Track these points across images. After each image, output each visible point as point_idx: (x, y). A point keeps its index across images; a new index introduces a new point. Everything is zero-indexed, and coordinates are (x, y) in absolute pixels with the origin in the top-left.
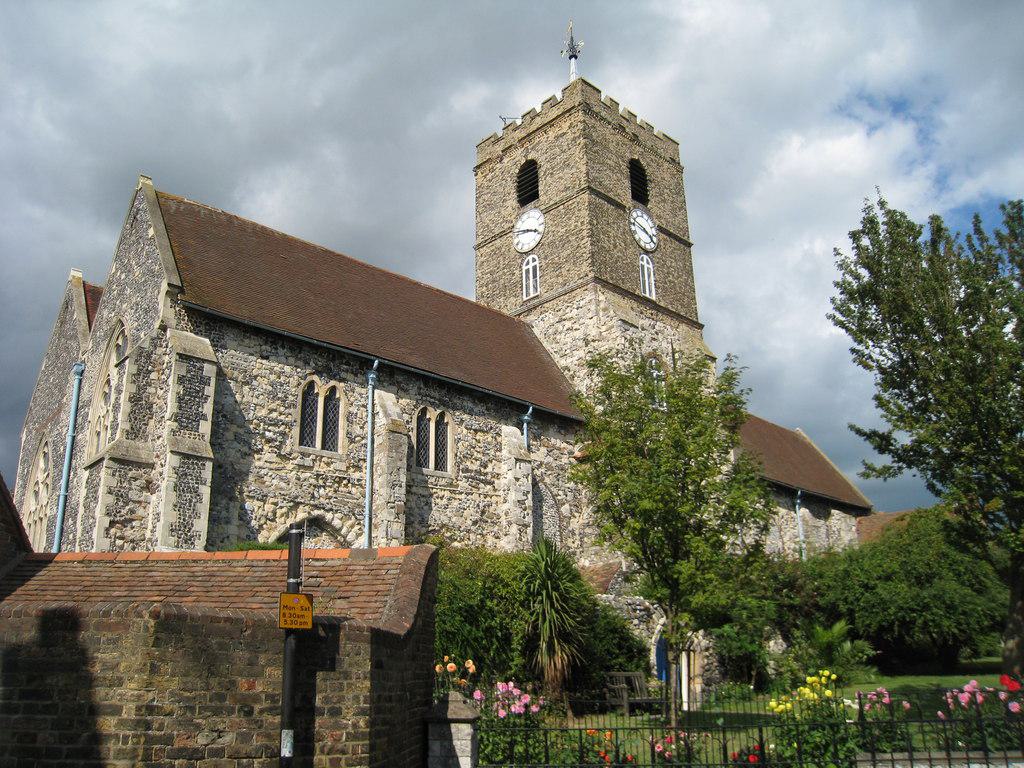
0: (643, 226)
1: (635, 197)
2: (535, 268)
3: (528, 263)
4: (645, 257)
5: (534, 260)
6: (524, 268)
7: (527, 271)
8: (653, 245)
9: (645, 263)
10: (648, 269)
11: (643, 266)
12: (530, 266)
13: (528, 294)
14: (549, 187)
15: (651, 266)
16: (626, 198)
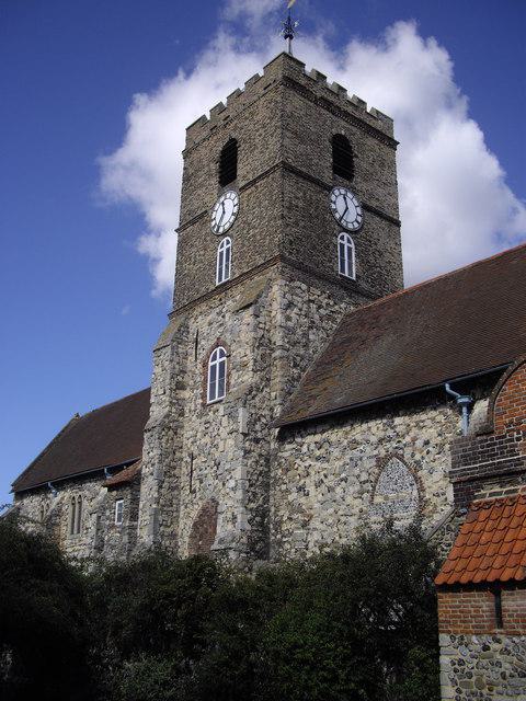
0: (345, 206)
1: (336, 170)
2: (228, 250)
3: (222, 247)
4: (346, 235)
5: (228, 242)
6: (219, 251)
7: (221, 254)
8: (356, 225)
9: (345, 242)
10: (349, 249)
11: (342, 246)
12: (224, 249)
13: (220, 279)
14: (244, 170)
15: (353, 246)
16: (327, 176)
